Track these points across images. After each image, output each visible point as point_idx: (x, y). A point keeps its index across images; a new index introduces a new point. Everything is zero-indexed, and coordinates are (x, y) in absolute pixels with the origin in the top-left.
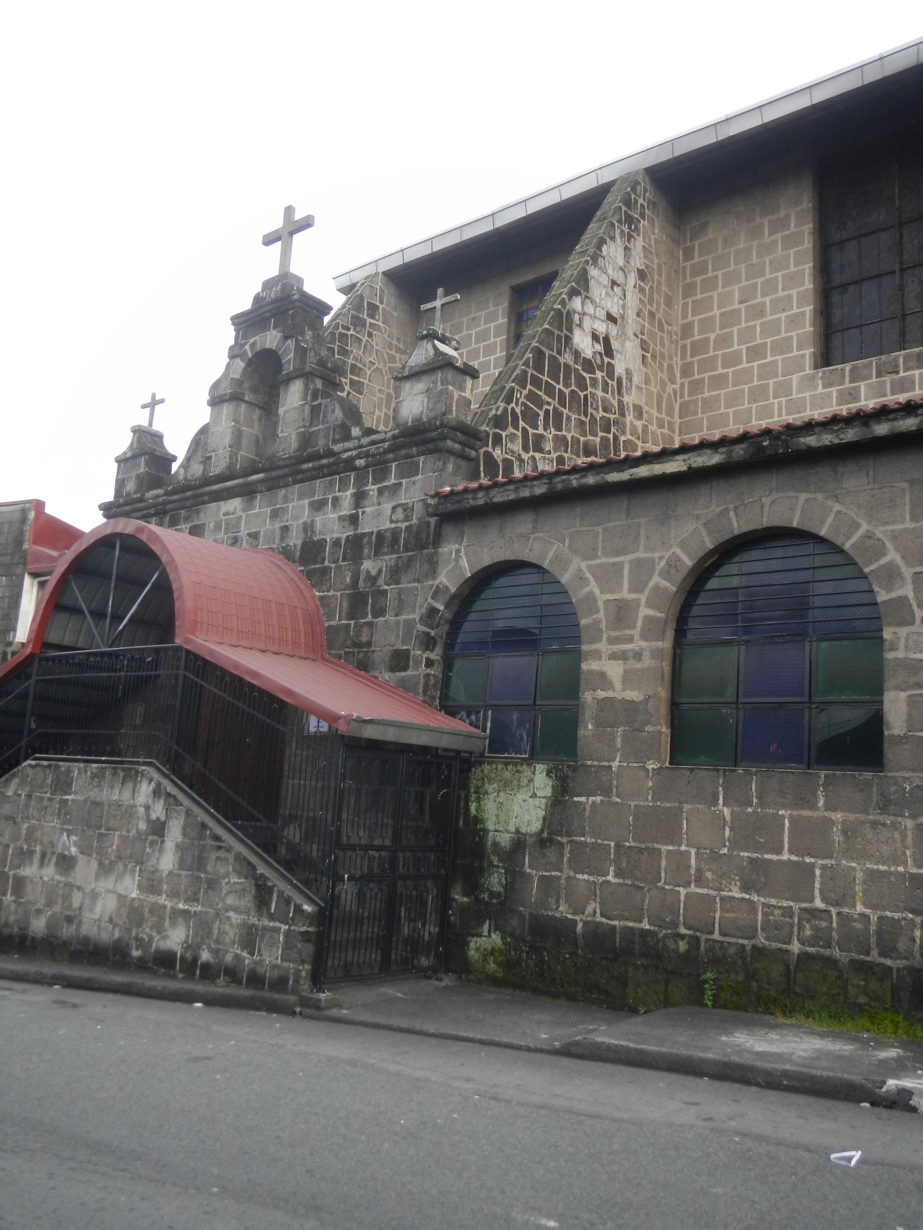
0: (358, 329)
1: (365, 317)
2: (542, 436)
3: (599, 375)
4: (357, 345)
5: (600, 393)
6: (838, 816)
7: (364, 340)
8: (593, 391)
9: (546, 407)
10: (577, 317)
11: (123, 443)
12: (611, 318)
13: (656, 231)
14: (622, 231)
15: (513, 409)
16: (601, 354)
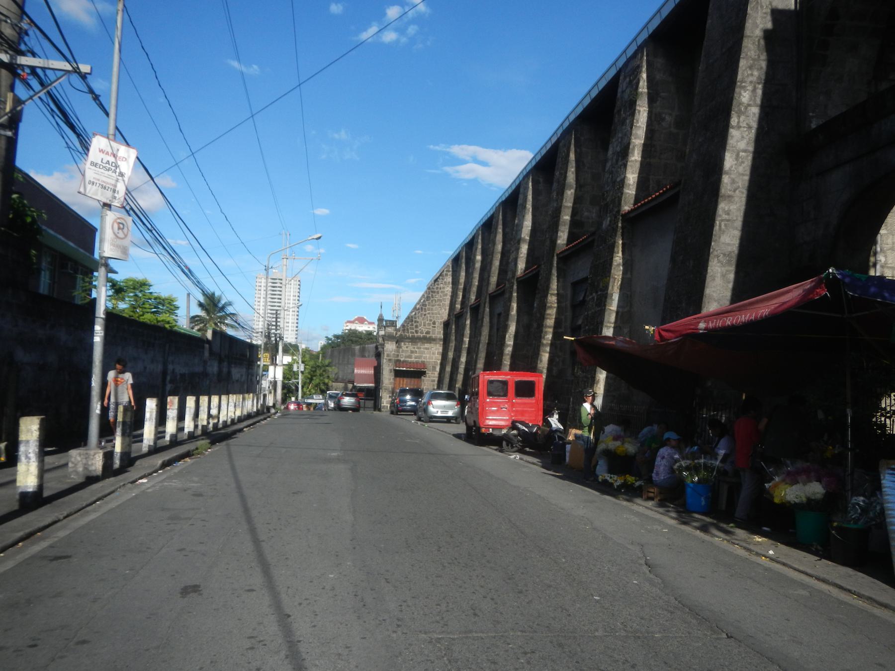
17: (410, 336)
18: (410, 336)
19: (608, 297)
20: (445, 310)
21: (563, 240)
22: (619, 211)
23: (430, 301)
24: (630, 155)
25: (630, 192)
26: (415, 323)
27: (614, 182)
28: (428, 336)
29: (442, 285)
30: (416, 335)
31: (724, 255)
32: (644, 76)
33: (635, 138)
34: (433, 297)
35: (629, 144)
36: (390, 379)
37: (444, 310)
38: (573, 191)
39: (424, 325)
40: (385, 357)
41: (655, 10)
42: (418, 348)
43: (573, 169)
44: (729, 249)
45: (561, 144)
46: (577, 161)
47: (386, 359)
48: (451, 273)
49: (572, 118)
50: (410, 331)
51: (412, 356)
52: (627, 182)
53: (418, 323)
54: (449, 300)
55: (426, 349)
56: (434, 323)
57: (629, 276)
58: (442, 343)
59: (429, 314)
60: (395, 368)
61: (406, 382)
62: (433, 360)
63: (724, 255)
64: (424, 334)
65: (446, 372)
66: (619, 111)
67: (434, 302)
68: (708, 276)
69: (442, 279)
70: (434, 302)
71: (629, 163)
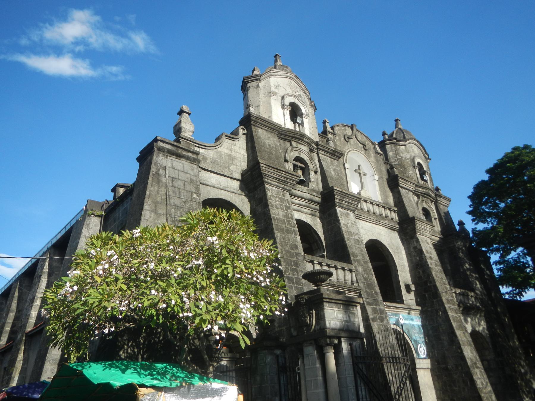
19: (12, 379)
21: (4, 342)
22: (25, 331)
24: (35, 302)
25: (32, 321)
27: (26, 315)
31: (53, 360)
32: (47, 264)
33: (38, 294)
35: (35, 297)
38: (14, 314)
41: (54, 235)
43: (16, 302)
44: (56, 357)
45: (13, 286)
46: (19, 297)
49: (20, 273)
52: (31, 316)
57: (26, 366)
63: (53, 360)
66: (36, 278)
68: (44, 370)
71: (33, 306)
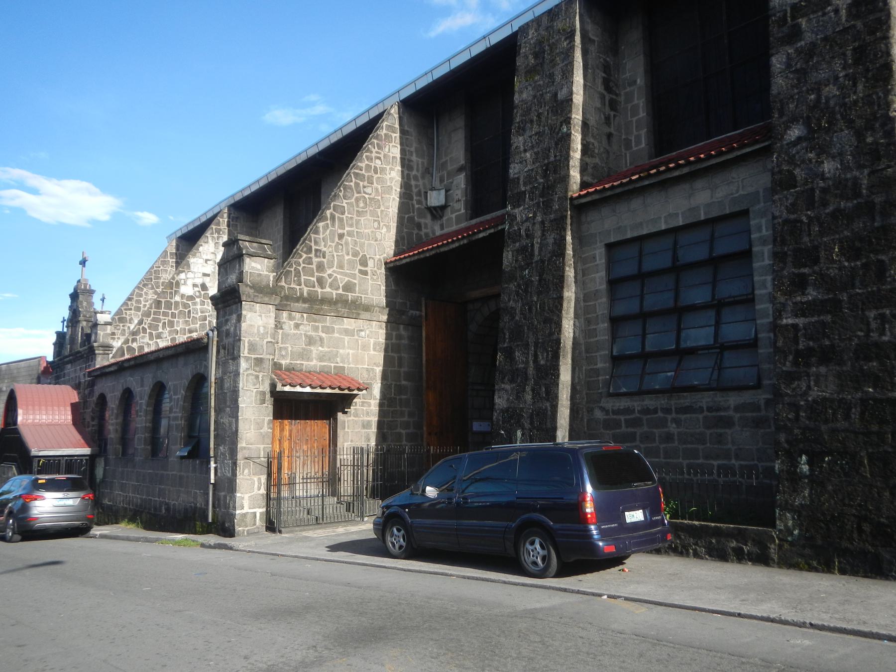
0: (165, 266)
1: (169, 259)
2: (162, 332)
3: (198, 300)
4: (165, 273)
5: (199, 307)
6: (130, 470)
7: (169, 270)
8: (194, 307)
9: (162, 321)
10: (182, 282)
11: (54, 338)
12: (205, 275)
13: (238, 229)
14: (213, 237)
15: (143, 327)
16: (199, 291)
17: (305, 294)
18: (306, 290)
20: (388, 228)
23: (353, 200)
26: (316, 256)
28: (350, 296)
29: (378, 161)
30: (319, 290)
34: (359, 192)
36: (259, 426)
37: (384, 230)
39: (341, 266)
40: (245, 352)
42: (328, 330)
47: (247, 359)
48: (398, 135)
50: (303, 278)
51: (311, 351)
53: (324, 257)
54: (397, 204)
55: (347, 332)
56: (364, 263)
58: (385, 318)
59: (350, 234)
60: (279, 388)
61: (291, 431)
62: (366, 366)
64: (340, 291)
65: (560, 386)
67: (362, 205)
69: (379, 147)
70: (362, 205)
